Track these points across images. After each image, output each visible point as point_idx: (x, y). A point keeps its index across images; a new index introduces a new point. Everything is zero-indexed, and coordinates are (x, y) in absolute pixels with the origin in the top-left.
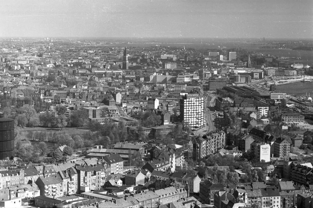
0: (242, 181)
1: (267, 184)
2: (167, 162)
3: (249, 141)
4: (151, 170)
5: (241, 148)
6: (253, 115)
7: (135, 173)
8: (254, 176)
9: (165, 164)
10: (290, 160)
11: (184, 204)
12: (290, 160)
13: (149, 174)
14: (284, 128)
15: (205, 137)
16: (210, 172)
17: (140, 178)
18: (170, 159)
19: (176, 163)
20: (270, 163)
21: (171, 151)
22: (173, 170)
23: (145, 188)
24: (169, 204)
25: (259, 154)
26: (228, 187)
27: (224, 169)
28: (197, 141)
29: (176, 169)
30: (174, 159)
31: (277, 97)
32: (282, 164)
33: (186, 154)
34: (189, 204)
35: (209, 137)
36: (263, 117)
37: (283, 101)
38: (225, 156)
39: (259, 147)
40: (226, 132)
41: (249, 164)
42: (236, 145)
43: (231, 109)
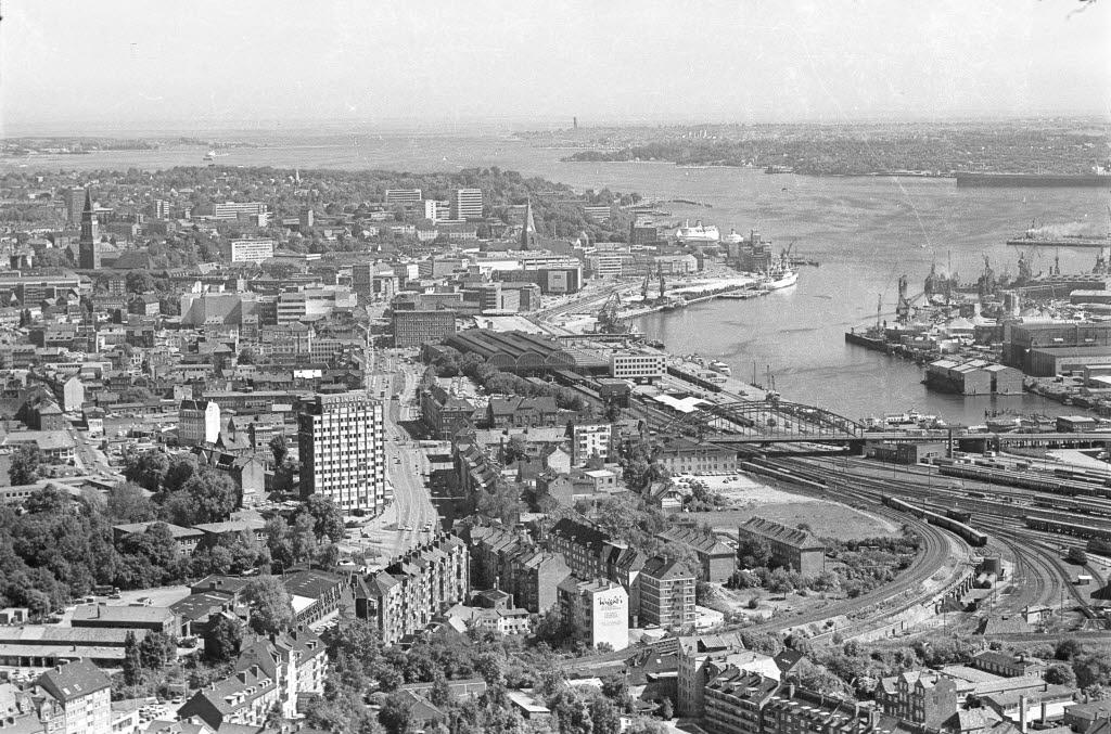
3: (552, 574)
5: (524, 597)
15: (394, 569)
25: (590, 623)
39: (588, 599)
40: (468, 540)
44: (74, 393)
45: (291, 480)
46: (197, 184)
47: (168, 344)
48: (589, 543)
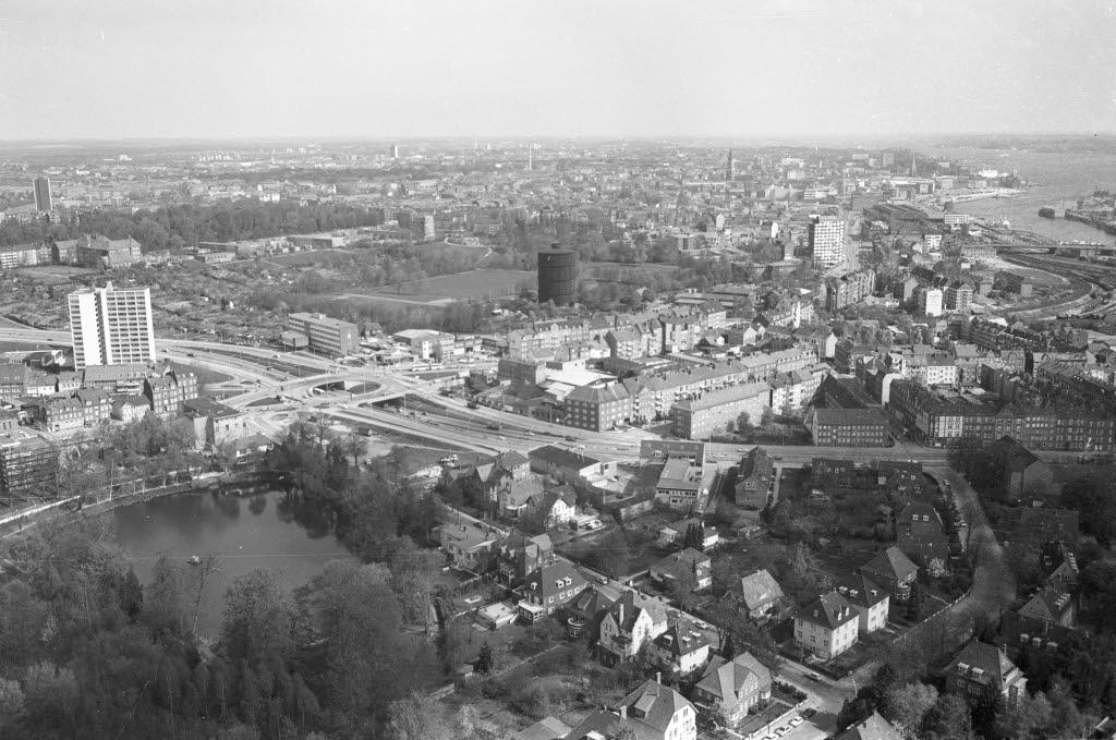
0: (898, 342)
1: (936, 348)
3: (910, 285)
4: (766, 324)
5: (898, 294)
7: (742, 329)
8: (916, 336)
9: (785, 317)
10: (973, 313)
11: (812, 373)
12: (973, 313)
13: (762, 330)
14: (965, 266)
15: (844, 278)
16: (850, 328)
17: (750, 335)
18: (793, 310)
19: (800, 314)
20: (941, 318)
22: (797, 325)
23: (756, 349)
24: (791, 373)
25: (925, 304)
27: (871, 324)
28: (832, 285)
29: (801, 324)
32: (960, 319)
33: (816, 303)
34: (820, 373)
38: (874, 307)
39: (925, 294)
41: (909, 318)
42: (890, 290)
44: (720, 220)
45: (806, 252)
46: (776, 153)
47: (761, 207)
48: (928, 277)
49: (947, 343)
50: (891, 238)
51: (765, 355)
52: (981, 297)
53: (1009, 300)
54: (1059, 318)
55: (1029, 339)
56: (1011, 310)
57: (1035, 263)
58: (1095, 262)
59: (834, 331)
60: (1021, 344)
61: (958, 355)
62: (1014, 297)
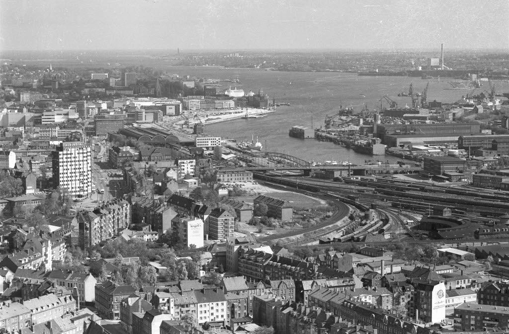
0: (162, 279)
2: (38, 255)
3: (169, 216)
4: (13, 268)
5: (156, 226)
6: (172, 174)
8: (180, 272)
9: (36, 259)
10: (237, 242)
11: (72, 321)
13: (10, 275)
14: (222, 192)
15: (97, 212)
16: (108, 266)
18: (44, 249)
19: (53, 255)
20: (204, 249)
21: (45, 236)
22: (49, 267)
24: (49, 323)
25: (186, 236)
26: (141, 290)
28: (84, 218)
29: (53, 266)
30: (49, 248)
31: (206, 143)
32: (224, 249)
33: (68, 240)
34: (82, 321)
35: (103, 211)
36: (187, 176)
37: (216, 149)
38: (131, 242)
40: (130, 203)
41: (171, 252)
42: (147, 223)
43: (136, 165)
49: (213, 277)
50: (143, 164)
51: (17, 305)
52: (242, 224)
53: (270, 226)
54: (321, 242)
55: (294, 268)
56: (274, 237)
57: (291, 186)
58: (348, 182)
59: (91, 271)
60: (290, 274)
61: (228, 290)
62: (275, 222)
